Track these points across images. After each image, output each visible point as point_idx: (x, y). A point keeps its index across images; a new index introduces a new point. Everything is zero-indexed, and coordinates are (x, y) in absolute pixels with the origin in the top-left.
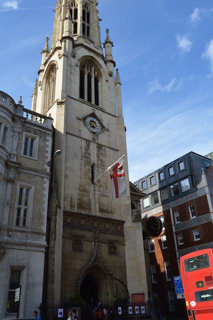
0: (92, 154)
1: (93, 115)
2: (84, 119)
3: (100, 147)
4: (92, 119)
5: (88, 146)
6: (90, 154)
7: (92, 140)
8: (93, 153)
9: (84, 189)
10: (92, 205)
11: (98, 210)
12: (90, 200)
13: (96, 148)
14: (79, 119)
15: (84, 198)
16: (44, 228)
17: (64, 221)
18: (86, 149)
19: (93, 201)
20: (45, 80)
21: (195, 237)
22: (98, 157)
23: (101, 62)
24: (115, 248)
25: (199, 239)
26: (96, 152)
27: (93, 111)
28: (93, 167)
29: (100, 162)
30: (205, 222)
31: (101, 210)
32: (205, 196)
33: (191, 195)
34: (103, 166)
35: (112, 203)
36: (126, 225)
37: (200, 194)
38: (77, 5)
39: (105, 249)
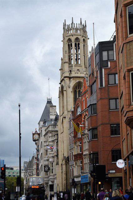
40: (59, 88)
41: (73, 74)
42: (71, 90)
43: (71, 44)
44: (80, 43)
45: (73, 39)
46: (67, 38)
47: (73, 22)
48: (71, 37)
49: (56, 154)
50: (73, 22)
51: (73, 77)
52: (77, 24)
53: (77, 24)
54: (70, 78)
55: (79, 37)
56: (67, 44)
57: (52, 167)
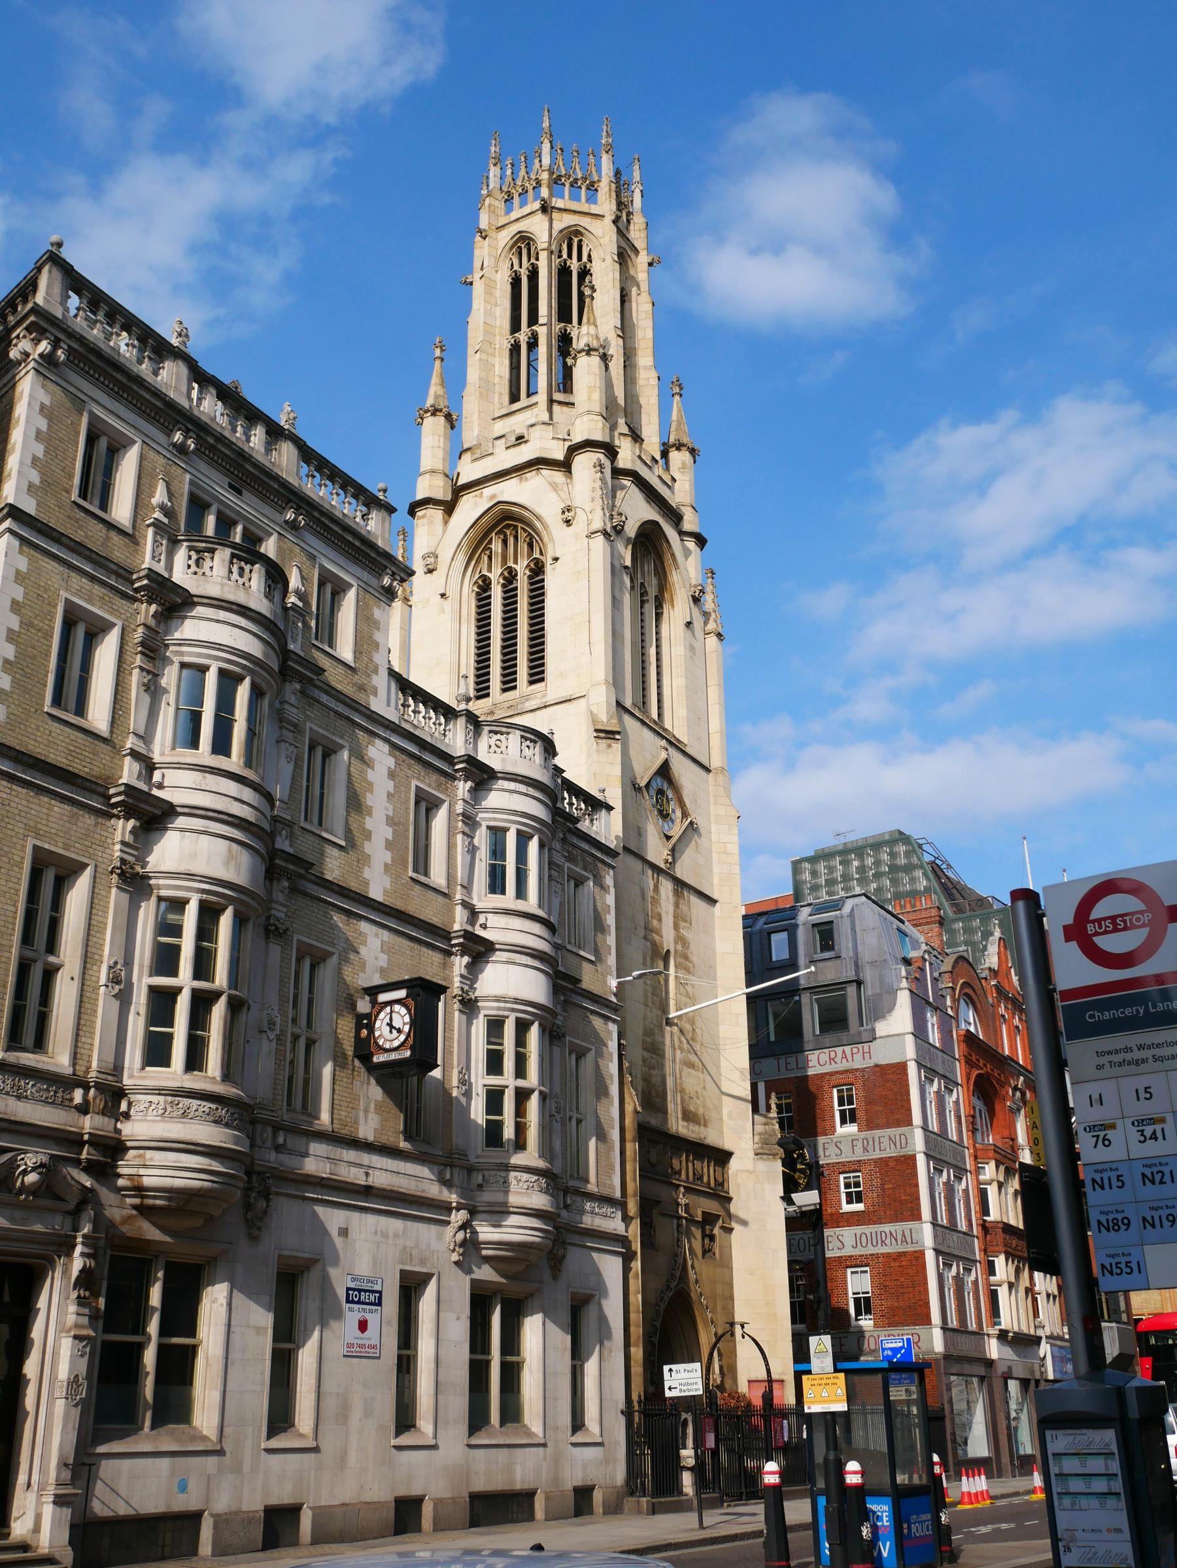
3: (681, 885)
7: (663, 866)
8: (667, 913)
9: (653, 1043)
13: (671, 894)
15: (653, 1072)
20: (461, 559)
21: (844, 1198)
22: (676, 927)
25: (859, 1207)
26: (671, 909)
27: (663, 755)
29: (679, 947)
30: (891, 1152)
32: (902, 1067)
33: (847, 1049)
34: (686, 958)
36: (734, 1164)
37: (882, 1054)
38: (590, 260)
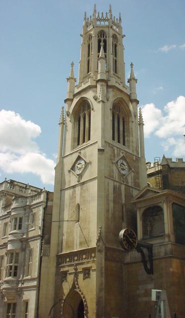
0: (77, 196)
1: (79, 158)
2: (73, 168)
4: (79, 162)
5: (75, 191)
6: (75, 197)
10: (75, 242)
11: (78, 244)
12: (74, 238)
14: (69, 171)
16: (35, 274)
17: (57, 263)
18: (73, 194)
19: (75, 238)
23: (89, 95)
24: (89, 274)
28: (79, 206)
31: (81, 244)
35: (89, 233)
39: (81, 276)
40: (63, 108)
41: (113, 82)
42: (109, 105)
43: (105, 42)
44: (118, 45)
45: (111, 32)
46: (98, 30)
47: (110, 11)
48: (106, 30)
49: (40, 232)
50: (110, 11)
51: (113, 87)
52: (114, 17)
53: (114, 17)
54: (108, 87)
55: (118, 35)
56: (97, 39)
57: (16, 262)
